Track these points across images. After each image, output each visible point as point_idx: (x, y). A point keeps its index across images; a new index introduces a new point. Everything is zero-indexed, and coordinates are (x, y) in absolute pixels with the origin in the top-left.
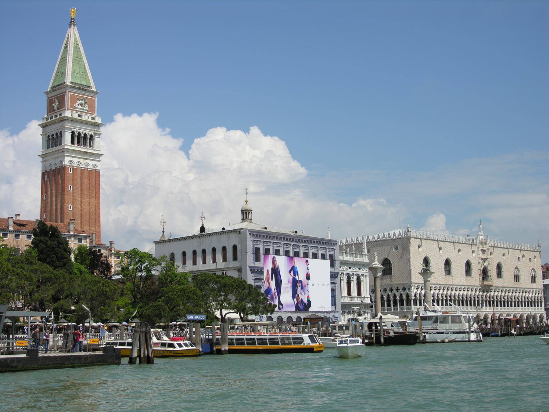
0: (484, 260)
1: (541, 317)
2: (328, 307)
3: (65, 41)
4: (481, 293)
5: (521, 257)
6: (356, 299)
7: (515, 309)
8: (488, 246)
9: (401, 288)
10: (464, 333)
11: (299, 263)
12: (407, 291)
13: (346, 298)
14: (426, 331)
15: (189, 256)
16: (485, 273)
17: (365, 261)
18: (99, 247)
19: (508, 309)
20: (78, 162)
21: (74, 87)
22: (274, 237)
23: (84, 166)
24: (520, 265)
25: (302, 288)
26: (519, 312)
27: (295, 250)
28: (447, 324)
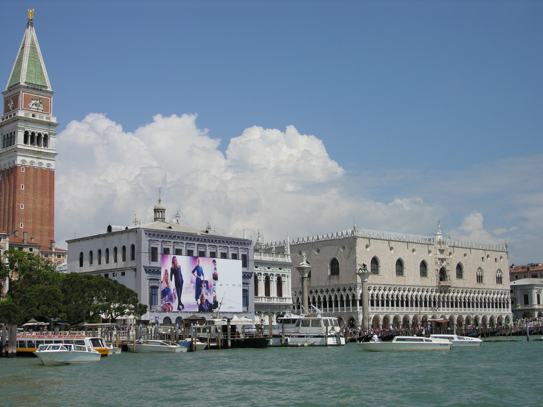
0: (442, 260)
1: (507, 318)
3: (23, 42)
4: (438, 294)
6: (275, 299)
9: (347, 289)
10: (322, 337)
11: (205, 264)
12: (353, 291)
13: (263, 299)
14: (289, 334)
15: (95, 254)
18: (30, 246)
19: (469, 310)
20: (31, 162)
21: (28, 87)
22: (174, 237)
23: (38, 166)
24: (483, 265)
25: (207, 289)
26: (481, 314)
27: (200, 250)
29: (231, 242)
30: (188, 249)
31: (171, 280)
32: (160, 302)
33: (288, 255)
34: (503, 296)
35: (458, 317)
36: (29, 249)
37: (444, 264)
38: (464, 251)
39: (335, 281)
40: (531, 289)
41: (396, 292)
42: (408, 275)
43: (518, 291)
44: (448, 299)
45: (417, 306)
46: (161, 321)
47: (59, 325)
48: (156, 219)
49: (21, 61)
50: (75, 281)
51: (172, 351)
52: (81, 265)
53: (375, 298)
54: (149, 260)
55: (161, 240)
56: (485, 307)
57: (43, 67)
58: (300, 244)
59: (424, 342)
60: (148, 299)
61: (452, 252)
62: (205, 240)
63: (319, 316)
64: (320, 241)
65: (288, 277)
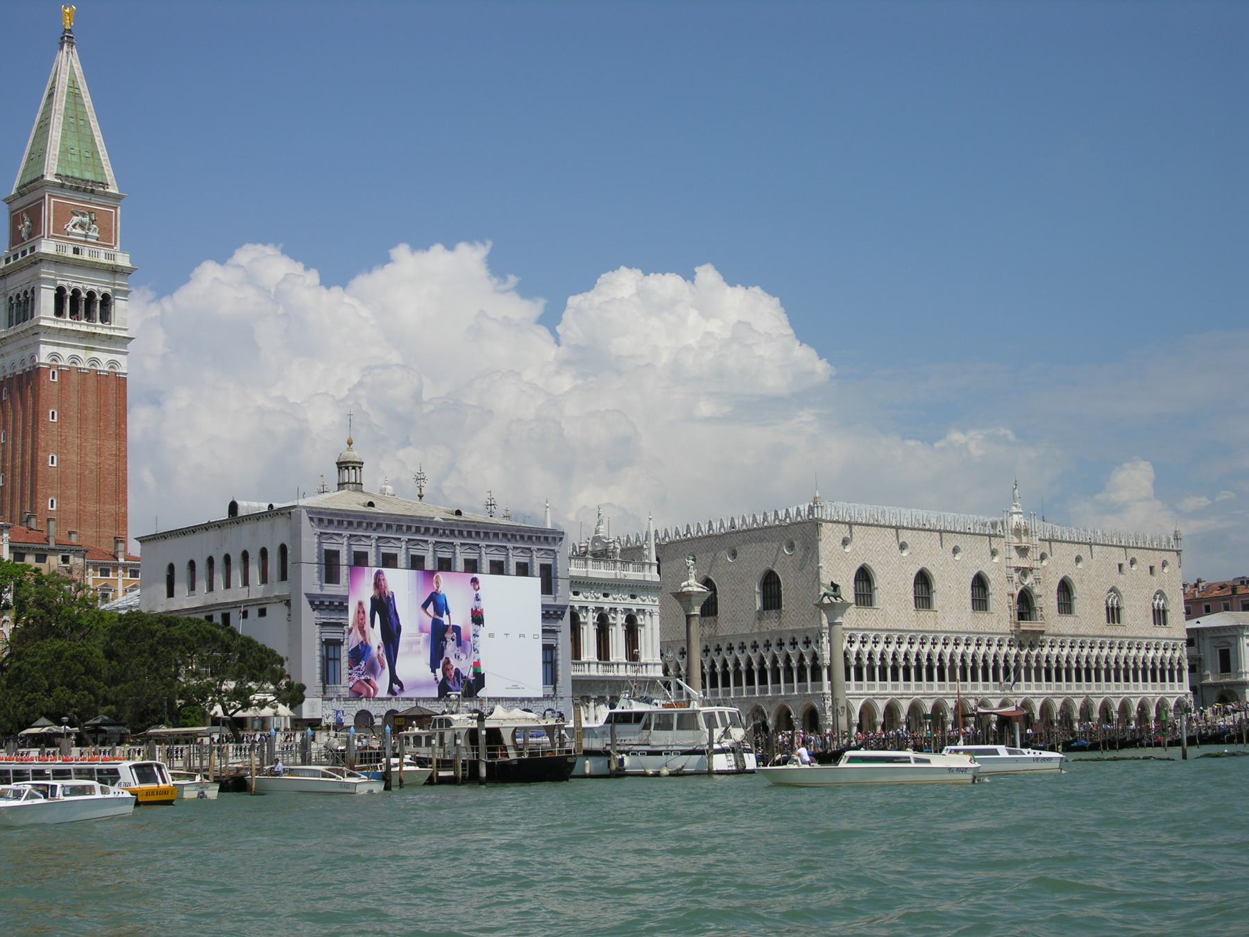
0: (1024, 572)
2: (536, 687)
3: (50, 82)
4: (1014, 651)
5: (1126, 564)
6: (622, 667)
7: (1108, 687)
8: (1035, 540)
9: (800, 641)
10: (702, 752)
11: (454, 588)
12: (813, 646)
13: (593, 667)
14: (626, 748)
15: (201, 568)
16: (1025, 604)
17: (648, 579)
18: (64, 551)
20: (73, 357)
21: (62, 186)
22: (379, 525)
23: (87, 366)
24: (1122, 582)
25: (459, 644)
26: (1117, 695)
27: (440, 555)
29: (514, 536)
30: (412, 552)
31: (372, 626)
32: (346, 678)
33: (651, 565)
34: (1169, 654)
38: (1076, 550)
39: (771, 624)
40: (1236, 637)
41: (916, 648)
43: (1207, 641)
44: (1037, 661)
46: (349, 721)
47: (105, 731)
48: (341, 485)
49: (48, 125)
50: (136, 629)
51: (347, 793)
52: (171, 593)
53: (866, 662)
55: (346, 533)
56: (1127, 679)
57: (97, 139)
58: (693, 539)
59: (913, 765)
60: (318, 671)
61: (1047, 551)
62: (452, 532)
63: (695, 706)
64: (738, 532)
65: (651, 615)
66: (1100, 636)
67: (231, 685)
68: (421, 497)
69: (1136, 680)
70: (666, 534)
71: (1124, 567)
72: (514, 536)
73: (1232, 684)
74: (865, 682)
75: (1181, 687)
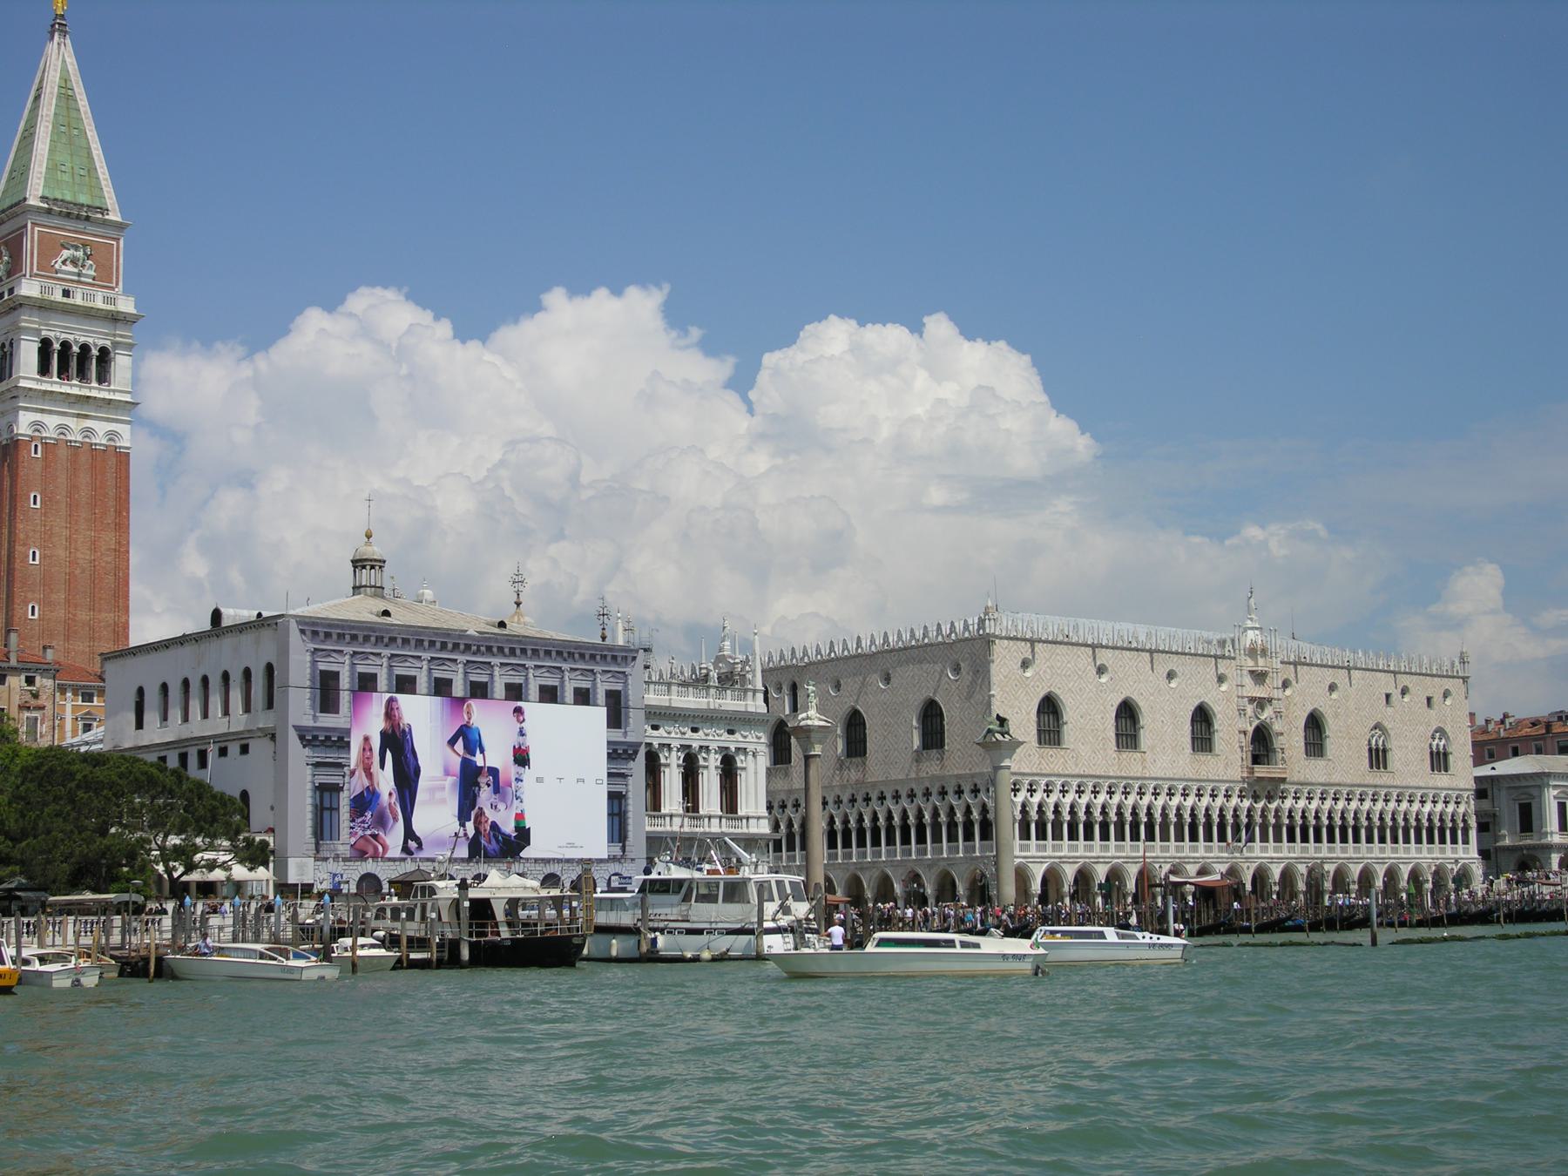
0: (1261, 703)
2: (596, 844)
3: (37, 81)
4: (1246, 803)
7: (1370, 850)
9: (967, 788)
10: (750, 932)
12: (982, 796)
14: (662, 925)
16: (1262, 744)
19: (1344, 850)
20: (60, 426)
21: (49, 211)
22: (393, 640)
23: (79, 438)
25: (497, 790)
26: (1381, 861)
27: (473, 678)
28: (713, 906)
29: (571, 655)
31: (382, 766)
32: (347, 832)
33: (755, 691)
35: (1311, 871)
36: (23, 678)
37: (1267, 714)
38: (1329, 676)
39: (931, 768)
40: (1540, 788)
41: (1117, 798)
42: (1153, 748)
43: (1504, 793)
44: (1277, 816)
45: (1180, 838)
47: (19, 898)
48: (357, 589)
49: (32, 135)
50: (52, 770)
51: (290, 979)
52: (139, 725)
54: (313, 707)
55: (349, 649)
56: (1395, 840)
57: (95, 152)
58: (837, 659)
59: (958, 950)
61: (1292, 677)
62: (489, 649)
63: (746, 872)
64: (892, 651)
66: (1359, 786)
67: (174, 840)
68: (518, 604)
69: (1407, 841)
70: (805, 653)
71: (1393, 699)
72: (571, 655)
73: (1533, 847)
74: (1050, 842)
75: (1466, 851)
